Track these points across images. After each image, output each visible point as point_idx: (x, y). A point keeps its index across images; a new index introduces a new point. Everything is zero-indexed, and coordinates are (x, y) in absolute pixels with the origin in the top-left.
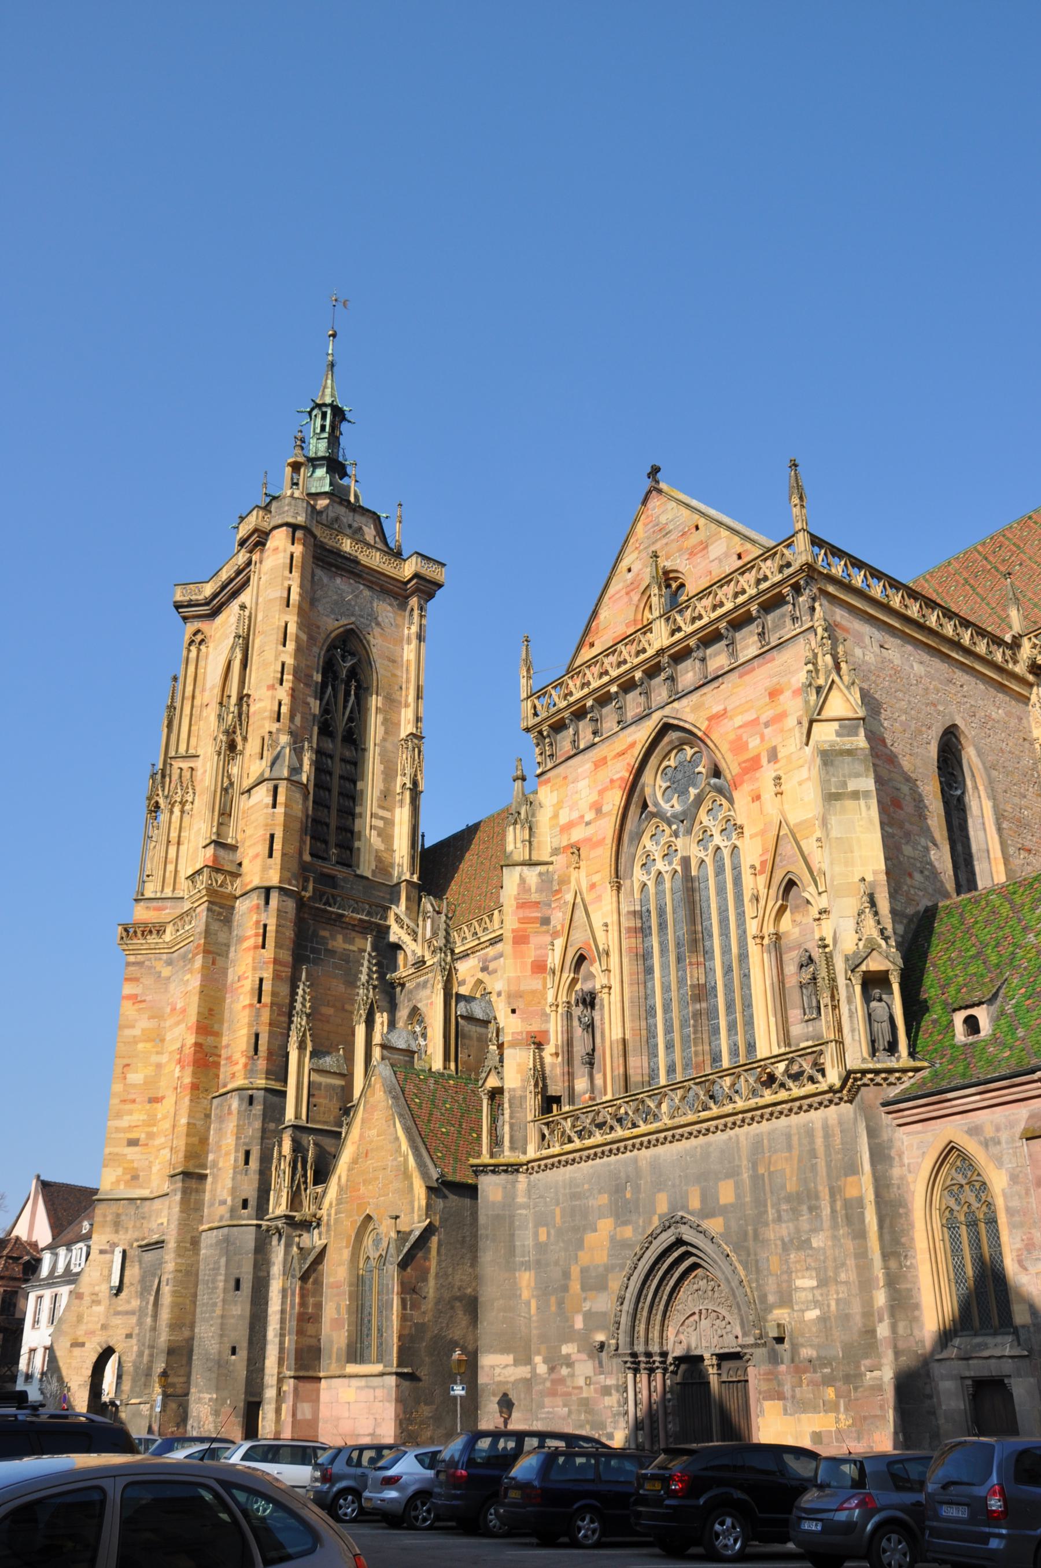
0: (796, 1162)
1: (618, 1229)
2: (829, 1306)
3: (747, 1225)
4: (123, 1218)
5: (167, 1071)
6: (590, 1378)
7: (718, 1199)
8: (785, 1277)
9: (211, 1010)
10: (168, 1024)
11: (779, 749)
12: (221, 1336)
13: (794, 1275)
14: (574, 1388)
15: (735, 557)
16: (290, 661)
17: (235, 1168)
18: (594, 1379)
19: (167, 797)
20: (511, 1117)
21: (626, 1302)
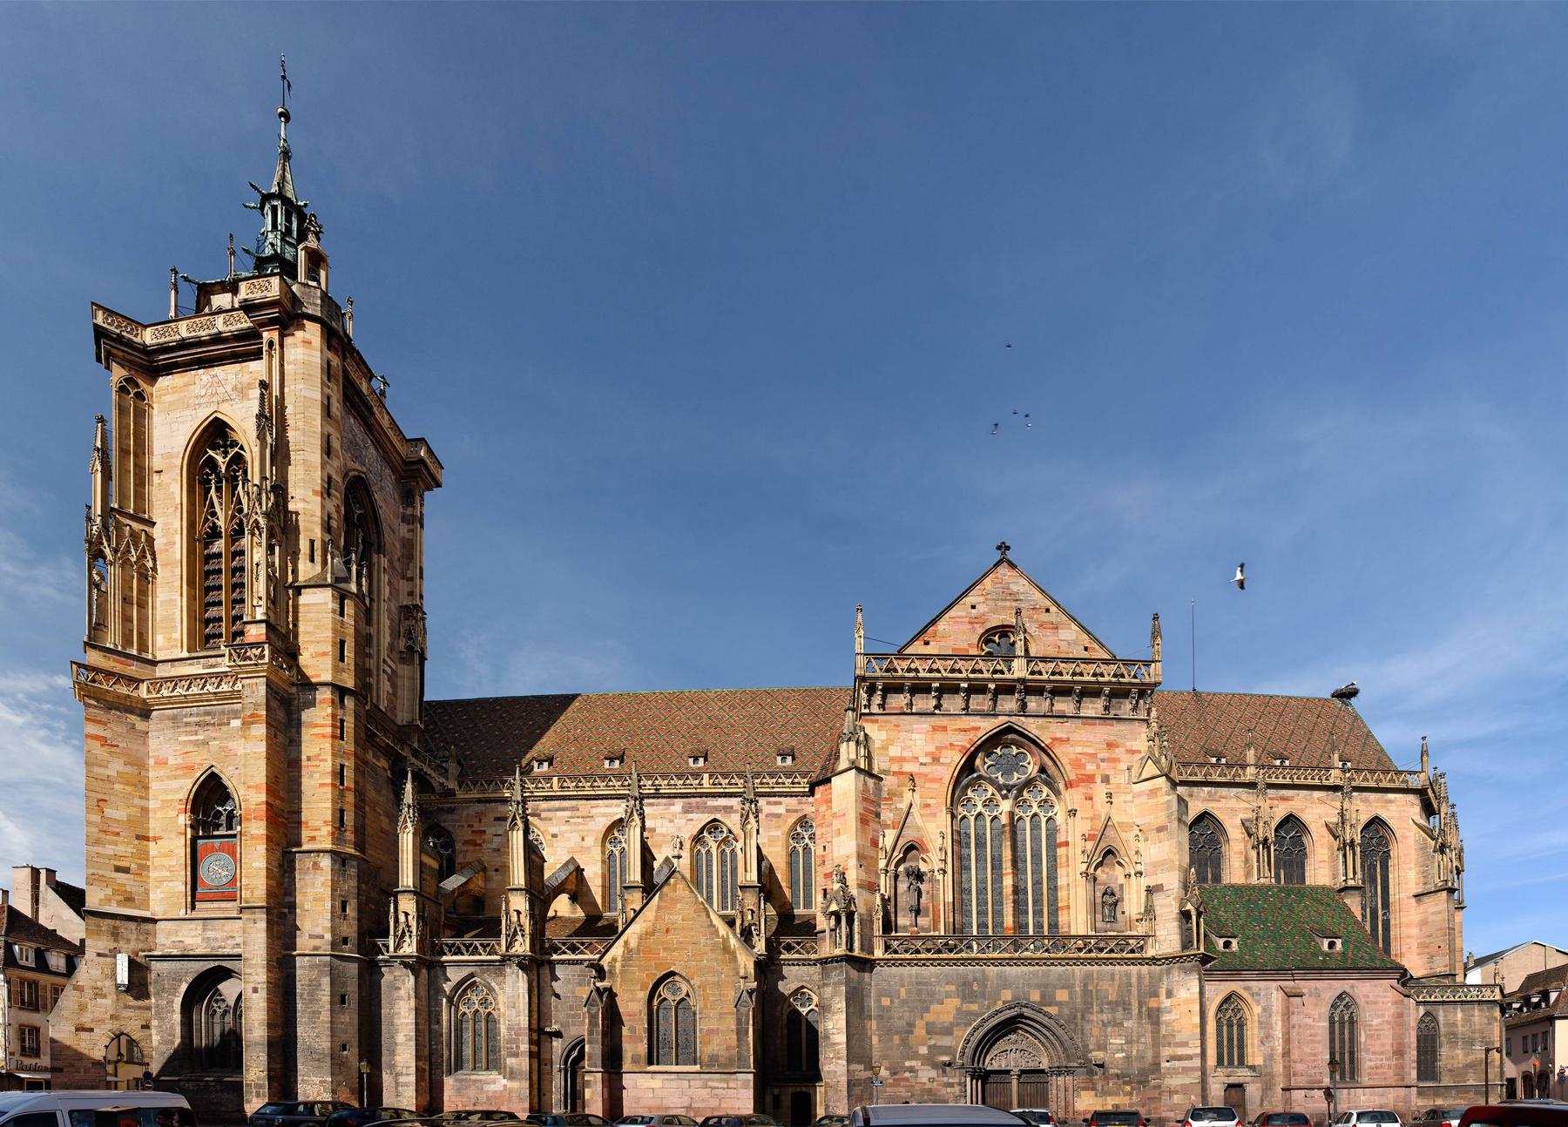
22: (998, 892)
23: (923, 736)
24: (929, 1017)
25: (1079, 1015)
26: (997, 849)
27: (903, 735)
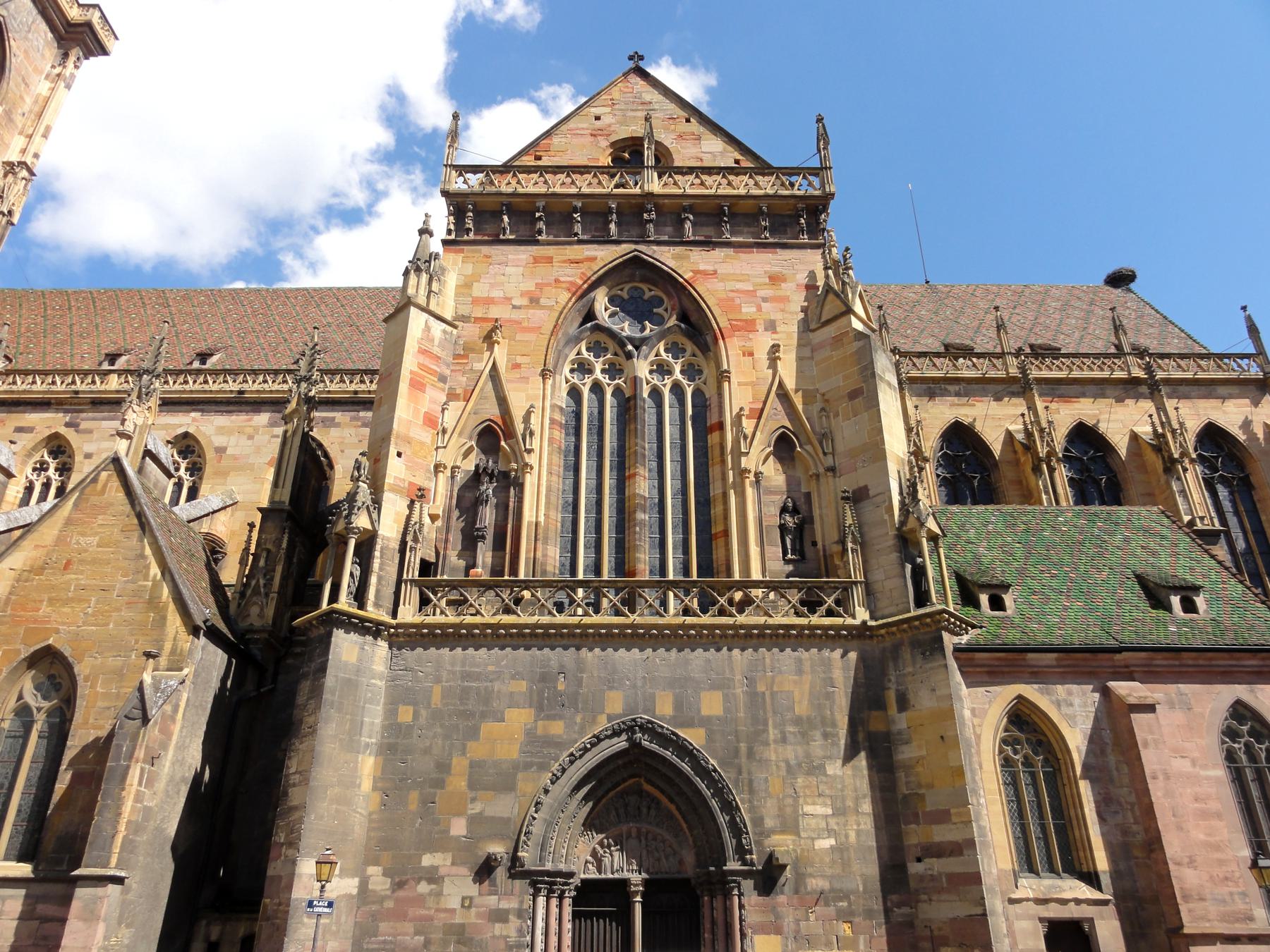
0: (807, 687)
1: (540, 723)
2: (847, 836)
3: (738, 741)
6: (471, 898)
7: (699, 711)
8: (789, 801)
11: (777, 323)
13: (801, 801)
14: (438, 910)
18: (477, 901)
20: (381, 569)
21: (544, 809)
23: (522, 269)
24: (477, 750)
25: (743, 746)
27: (494, 269)
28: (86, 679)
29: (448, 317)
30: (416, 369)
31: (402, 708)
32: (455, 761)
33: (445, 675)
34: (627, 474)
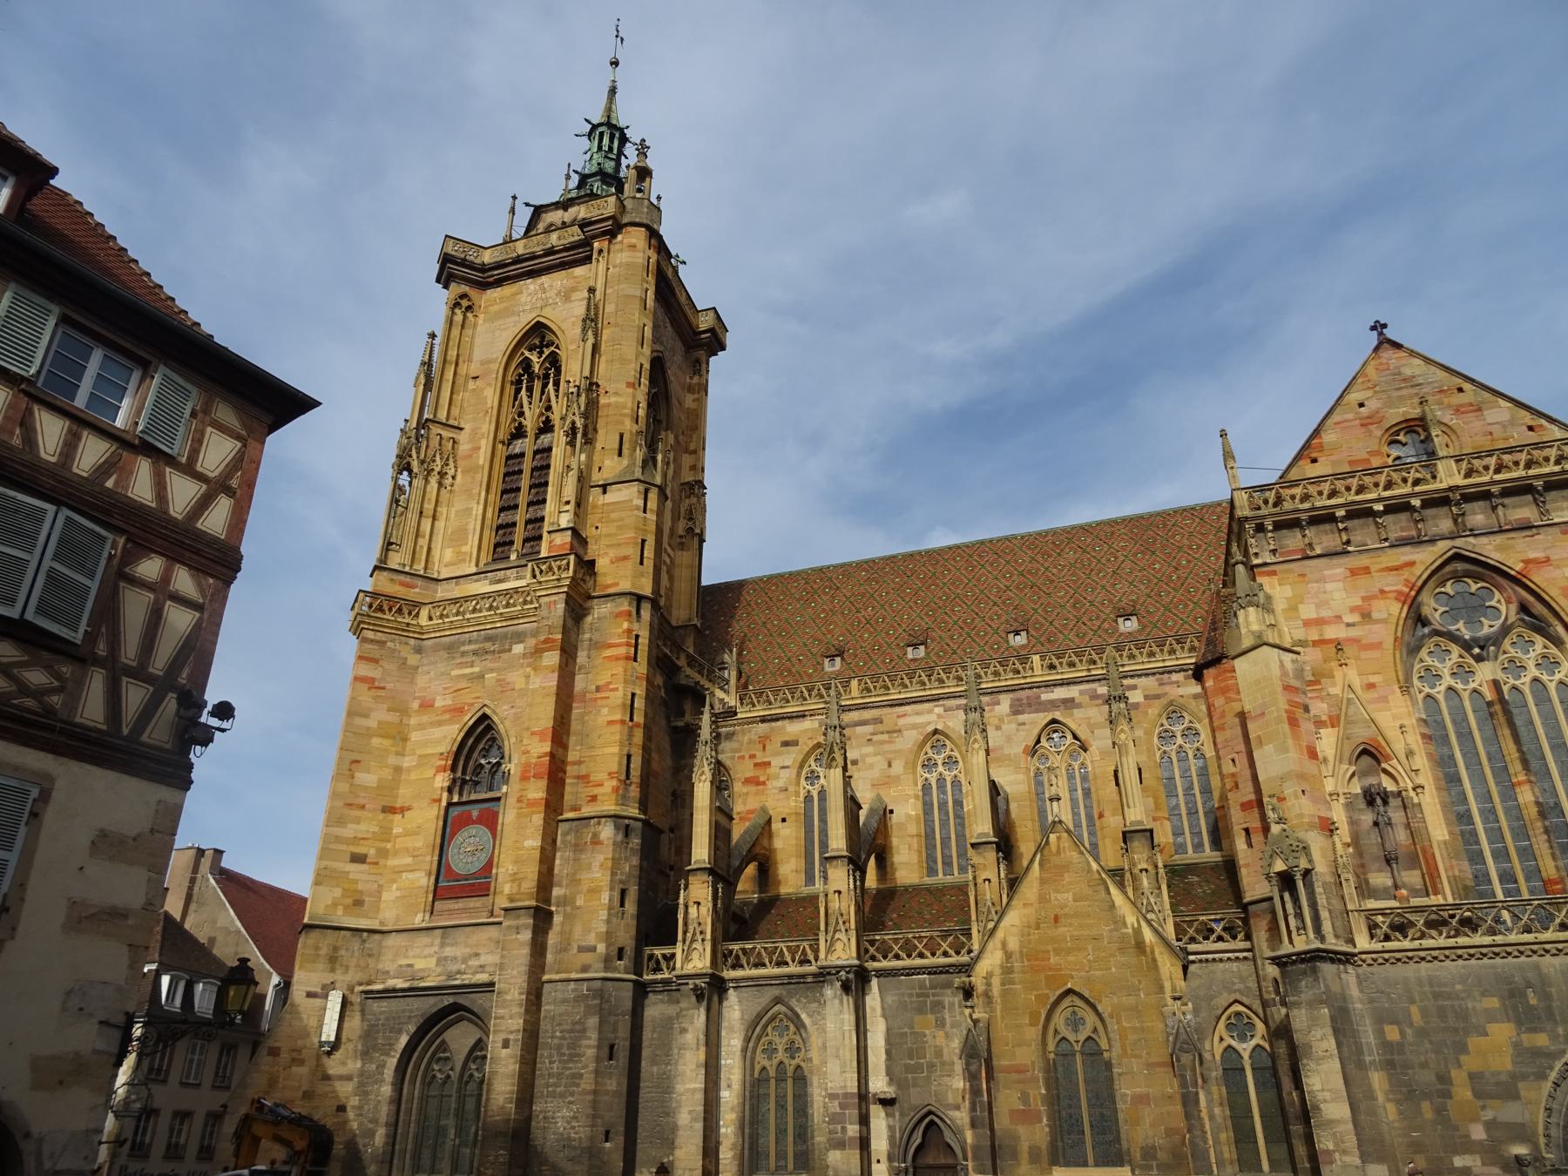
1: (1524, 1036)
4: (342, 952)
5: (413, 776)
9: (562, 717)
10: (413, 721)
12: (594, 1117)
15: (1525, 428)
16: (647, 366)
17: (610, 908)
19: (423, 462)
22: (1516, 813)
24: (1470, 1062)
26: (1493, 740)
28: (1111, 1016)
29: (1288, 646)
30: (1287, 707)
31: (1387, 1028)
32: (1454, 1073)
33: (1416, 995)
34: (1514, 780)
